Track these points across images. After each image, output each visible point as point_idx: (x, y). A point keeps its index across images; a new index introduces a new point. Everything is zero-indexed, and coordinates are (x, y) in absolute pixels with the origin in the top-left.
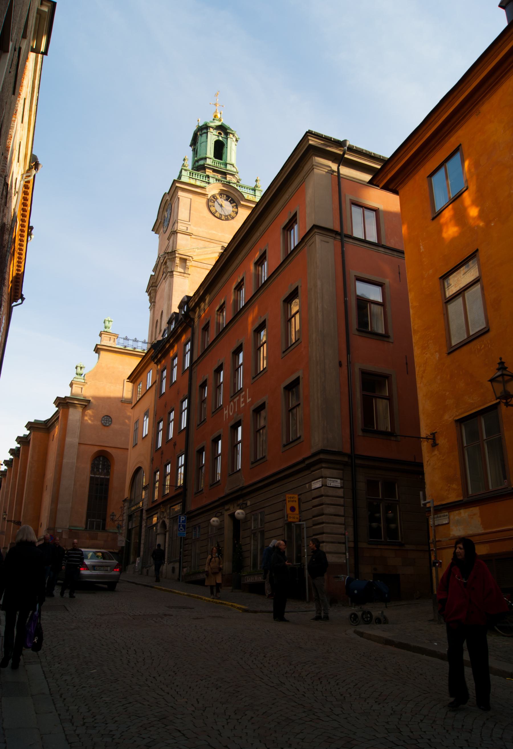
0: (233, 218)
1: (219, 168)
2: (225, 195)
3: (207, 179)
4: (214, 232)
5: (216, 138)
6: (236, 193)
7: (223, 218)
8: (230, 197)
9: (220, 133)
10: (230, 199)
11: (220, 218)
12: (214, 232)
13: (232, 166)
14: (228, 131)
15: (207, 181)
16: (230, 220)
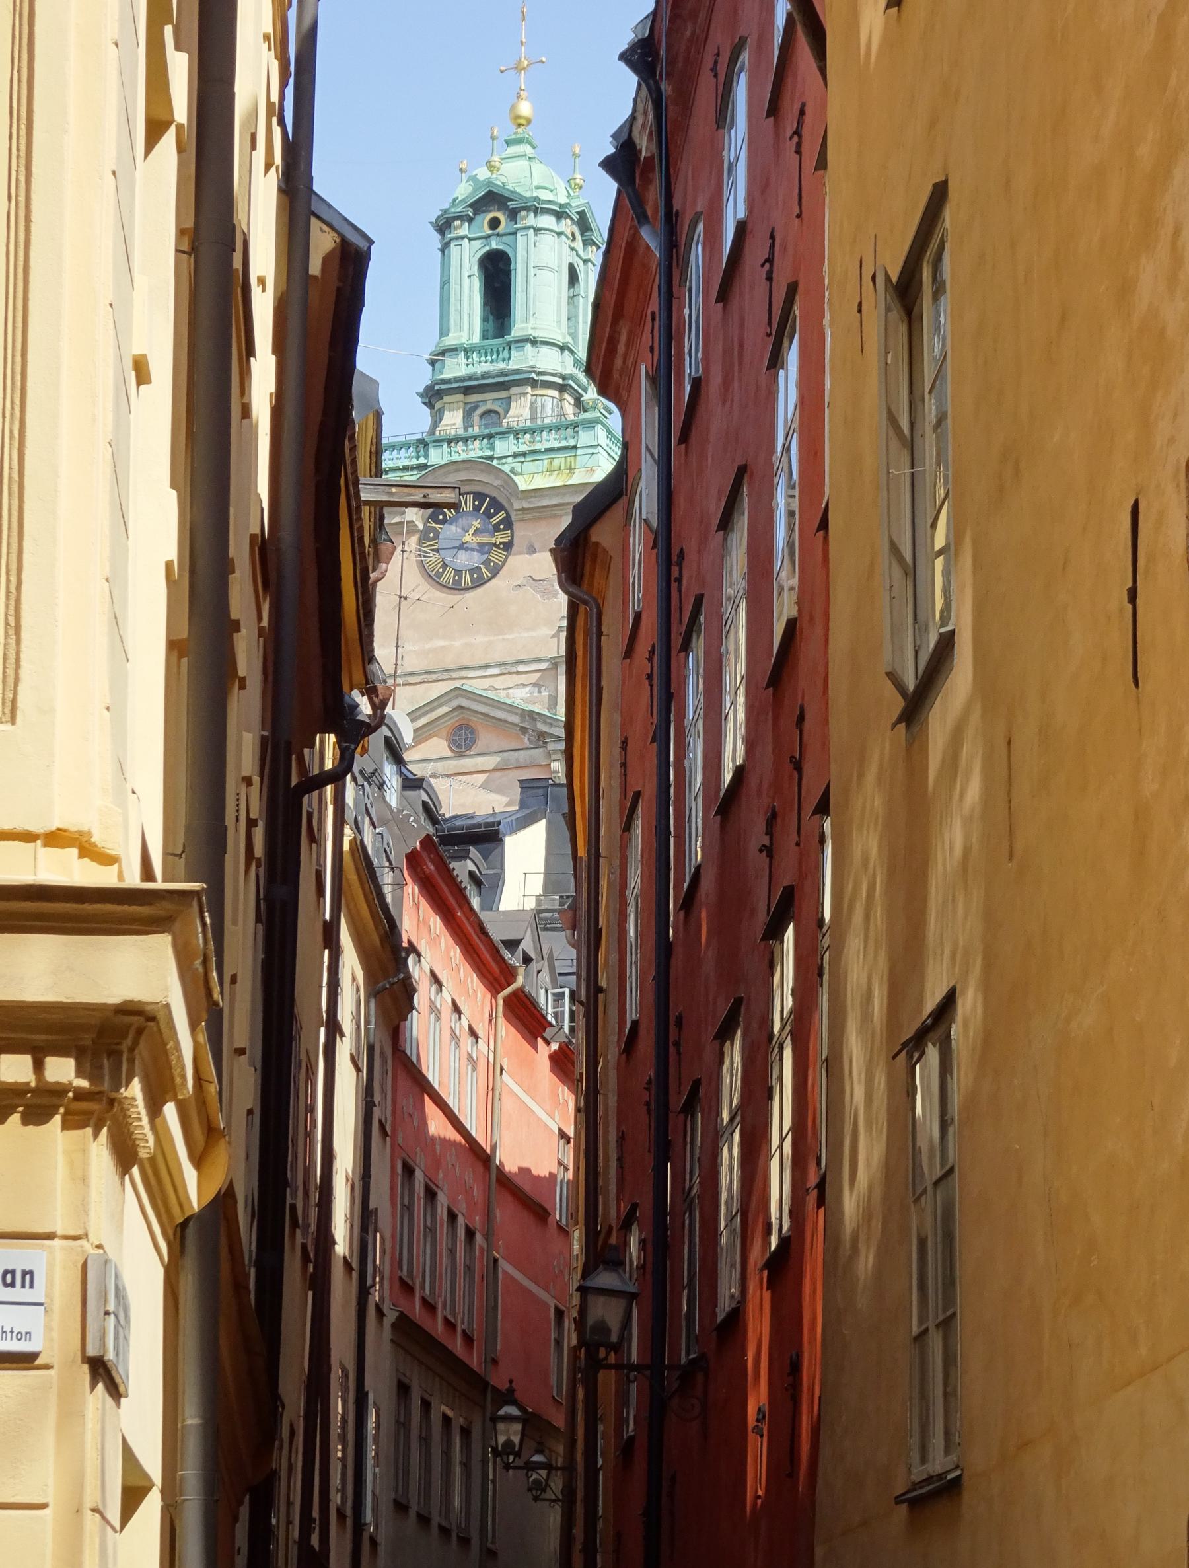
0: (495, 571)
1: (477, 379)
2: (469, 493)
3: (422, 452)
4: (441, 643)
5: (478, 249)
6: (497, 478)
7: (467, 579)
8: (486, 496)
9: (495, 223)
10: (488, 499)
11: (457, 587)
12: (441, 643)
13: (529, 345)
14: (512, 204)
15: (422, 460)
16: (490, 579)
